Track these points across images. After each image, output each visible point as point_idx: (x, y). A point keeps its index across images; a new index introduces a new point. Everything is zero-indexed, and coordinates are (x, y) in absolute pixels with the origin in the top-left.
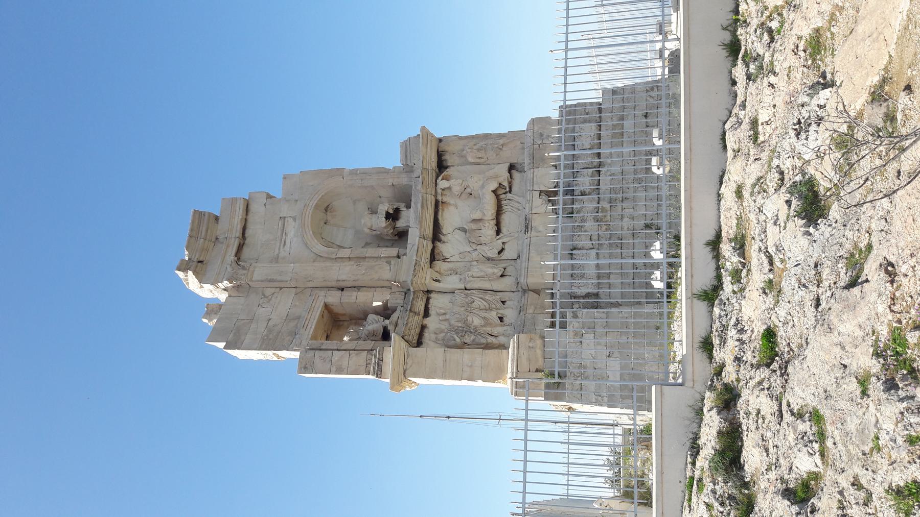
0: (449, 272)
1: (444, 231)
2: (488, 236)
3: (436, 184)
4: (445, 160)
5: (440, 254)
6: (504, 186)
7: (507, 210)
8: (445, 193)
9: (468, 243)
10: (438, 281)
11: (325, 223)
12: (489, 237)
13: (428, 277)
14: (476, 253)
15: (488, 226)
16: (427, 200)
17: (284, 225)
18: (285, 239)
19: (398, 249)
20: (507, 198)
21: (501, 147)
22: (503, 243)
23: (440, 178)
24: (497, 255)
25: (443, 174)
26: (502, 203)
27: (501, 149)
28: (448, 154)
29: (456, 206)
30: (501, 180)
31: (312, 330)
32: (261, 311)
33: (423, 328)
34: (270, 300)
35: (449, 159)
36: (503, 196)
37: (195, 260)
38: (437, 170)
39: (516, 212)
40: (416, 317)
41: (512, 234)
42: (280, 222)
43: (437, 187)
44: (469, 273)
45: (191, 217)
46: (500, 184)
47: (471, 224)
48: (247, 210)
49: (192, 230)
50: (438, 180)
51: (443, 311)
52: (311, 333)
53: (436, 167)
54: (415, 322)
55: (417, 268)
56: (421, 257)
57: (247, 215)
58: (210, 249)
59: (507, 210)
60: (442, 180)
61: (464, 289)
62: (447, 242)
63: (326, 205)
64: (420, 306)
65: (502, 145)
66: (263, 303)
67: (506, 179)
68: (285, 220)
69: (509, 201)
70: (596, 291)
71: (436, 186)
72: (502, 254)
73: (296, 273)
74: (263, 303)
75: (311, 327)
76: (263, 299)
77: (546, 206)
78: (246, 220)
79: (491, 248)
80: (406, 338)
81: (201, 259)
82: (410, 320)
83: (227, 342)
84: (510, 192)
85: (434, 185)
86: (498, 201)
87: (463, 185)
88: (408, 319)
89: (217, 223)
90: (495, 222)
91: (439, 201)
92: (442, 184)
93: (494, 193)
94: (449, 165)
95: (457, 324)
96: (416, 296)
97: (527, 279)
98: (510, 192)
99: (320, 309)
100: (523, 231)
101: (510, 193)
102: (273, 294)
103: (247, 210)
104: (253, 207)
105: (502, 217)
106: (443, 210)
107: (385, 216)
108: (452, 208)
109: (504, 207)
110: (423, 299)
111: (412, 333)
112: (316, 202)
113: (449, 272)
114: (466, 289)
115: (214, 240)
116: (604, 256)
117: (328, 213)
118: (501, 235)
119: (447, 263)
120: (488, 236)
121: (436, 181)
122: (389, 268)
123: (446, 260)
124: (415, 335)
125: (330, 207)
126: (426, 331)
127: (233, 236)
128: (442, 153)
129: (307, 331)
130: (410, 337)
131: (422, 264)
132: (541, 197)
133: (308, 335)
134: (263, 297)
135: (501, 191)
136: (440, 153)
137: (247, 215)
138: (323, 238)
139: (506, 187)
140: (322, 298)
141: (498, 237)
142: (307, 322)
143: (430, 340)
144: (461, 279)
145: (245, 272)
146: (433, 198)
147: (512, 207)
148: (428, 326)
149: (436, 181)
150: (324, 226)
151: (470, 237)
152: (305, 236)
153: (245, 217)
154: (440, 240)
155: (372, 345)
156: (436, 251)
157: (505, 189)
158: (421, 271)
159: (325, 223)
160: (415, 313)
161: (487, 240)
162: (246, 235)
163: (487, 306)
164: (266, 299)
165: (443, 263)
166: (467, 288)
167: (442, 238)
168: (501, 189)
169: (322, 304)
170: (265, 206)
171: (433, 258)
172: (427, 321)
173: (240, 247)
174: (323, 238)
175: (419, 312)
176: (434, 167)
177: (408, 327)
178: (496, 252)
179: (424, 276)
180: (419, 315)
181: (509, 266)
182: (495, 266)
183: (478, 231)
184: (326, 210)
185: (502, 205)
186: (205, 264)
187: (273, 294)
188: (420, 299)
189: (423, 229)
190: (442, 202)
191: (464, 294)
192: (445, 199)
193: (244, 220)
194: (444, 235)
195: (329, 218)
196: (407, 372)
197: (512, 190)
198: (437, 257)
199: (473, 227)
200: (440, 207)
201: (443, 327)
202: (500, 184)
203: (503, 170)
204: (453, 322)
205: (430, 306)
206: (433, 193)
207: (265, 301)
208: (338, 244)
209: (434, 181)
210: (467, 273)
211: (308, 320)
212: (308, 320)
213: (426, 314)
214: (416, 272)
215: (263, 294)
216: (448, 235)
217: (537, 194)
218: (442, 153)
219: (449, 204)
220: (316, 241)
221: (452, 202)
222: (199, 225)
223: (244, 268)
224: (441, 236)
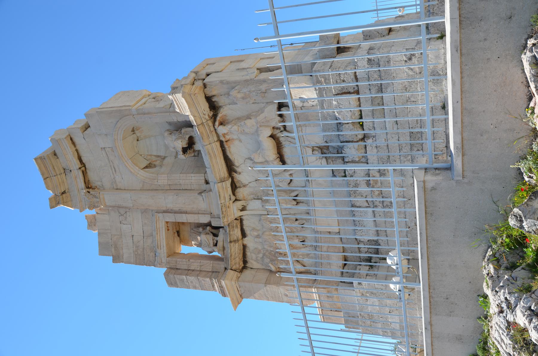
0: (252, 196)
1: (236, 164)
3: (215, 129)
4: (215, 101)
10: (243, 209)
11: (138, 140)
13: (235, 211)
16: (212, 148)
17: (107, 154)
18: (114, 166)
19: (203, 175)
21: (265, 91)
23: (217, 123)
25: (218, 118)
26: (280, 140)
27: (265, 93)
29: (240, 141)
30: (273, 124)
31: (165, 248)
32: (124, 227)
33: (244, 247)
34: (126, 218)
35: (220, 100)
37: (59, 194)
40: (236, 245)
42: (103, 152)
45: (36, 165)
46: (273, 128)
48: (74, 143)
49: (43, 174)
50: (215, 127)
51: (256, 234)
52: (165, 251)
54: (237, 250)
55: (224, 210)
56: (225, 198)
57: (75, 146)
58: (65, 180)
62: (242, 172)
63: (131, 130)
64: (237, 233)
65: (266, 90)
66: (122, 220)
68: (105, 150)
70: (375, 238)
73: (135, 201)
74: (122, 220)
75: (163, 246)
76: (121, 217)
77: (320, 161)
78: (77, 150)
80: (234, 268)
81: (63, 191)
82: (233, 250)
83: (112, 256)
85: (214, 133)
87: (240, 131)
88: (231, 251)
89: (58, 158)
90: (279, 159)
92: (222, 130)
94: (220, 105)
95: (269, 249)
96: (230, 227)
99: (164, 228)
102: (126, 212)
103: (74, 143)
104: (76, 140)
105: (283, 151)
106: (229, 147)
107: (182, 153)
108: (237, 143)
109: (283, 143)
110: (237, 226)
111: (237, 261)
112: (122, 136)
113: (252, 196)
115: (62, 171)
116: (380, 215)
117: (136, 132)
122: (202, 199)
124: (240, 261)
125: (135, 127)
126: (247, 248)
127: (75, 169)
129: (162, 250)
130: (237, 265)
131: (227, 203)
132: (314, 153)
133: (164, 253)
134: (120, 215)
135: (276, 132)
137: (75, 146)
138: (141, 155)
140: (163, 219)
142: (159, 243)
143: (252, 259)
145: (98, 200)
146: (218, 144)
148: (247, 245)
150: (137, 144)
152: (127, 165)
153: (74, 149)
154: (236, 172)
155: (211, 265)
156: (235, 180)
158: (228, 209)
159: (138, 140)
160: (235, 241)
162: (84, 161)
163: (290, 231)
164: (122, 216)
167: (238, 170)
169: (164, 223)
170: (84, 139)
171: (234, 187)
172: (246, 241)
173: (84, 173)
174: (141, 155)
175: (238, 238)
176: (207, 117)
177: (233, 257)
178: (286, 184)
179: (232, 212)
180: (238, 240)
181: (300, 192)
184: (133, 131)
185: (280, 141)
186: (68, 192)
187: (126, 212)
188: (235, 228)
189: (217, 175)
191: (269, 221)
192: (228, 137)
193: (76, 152)
194: (237, 167)
195: (138, 135)
196: (242, 295)
198: (238, 185)
200: (226, 146)
201: (260, 247)
203: (272, 112)
204: (266, 247)
205: (244, 228)
206: (216, 139)
207: (123, 219)
208: (155, 154)
209: (212, 129)
211: (159, 240)
212: (159, 240)
213: (244, 235)
214: (224, 213)
215: (119, 213)
217: (310, 151)
219: (233, 139)
220: (137, 168)
221: (235, 137)
222: (46, 168)
223: (95, 197)
224: (235, 168)
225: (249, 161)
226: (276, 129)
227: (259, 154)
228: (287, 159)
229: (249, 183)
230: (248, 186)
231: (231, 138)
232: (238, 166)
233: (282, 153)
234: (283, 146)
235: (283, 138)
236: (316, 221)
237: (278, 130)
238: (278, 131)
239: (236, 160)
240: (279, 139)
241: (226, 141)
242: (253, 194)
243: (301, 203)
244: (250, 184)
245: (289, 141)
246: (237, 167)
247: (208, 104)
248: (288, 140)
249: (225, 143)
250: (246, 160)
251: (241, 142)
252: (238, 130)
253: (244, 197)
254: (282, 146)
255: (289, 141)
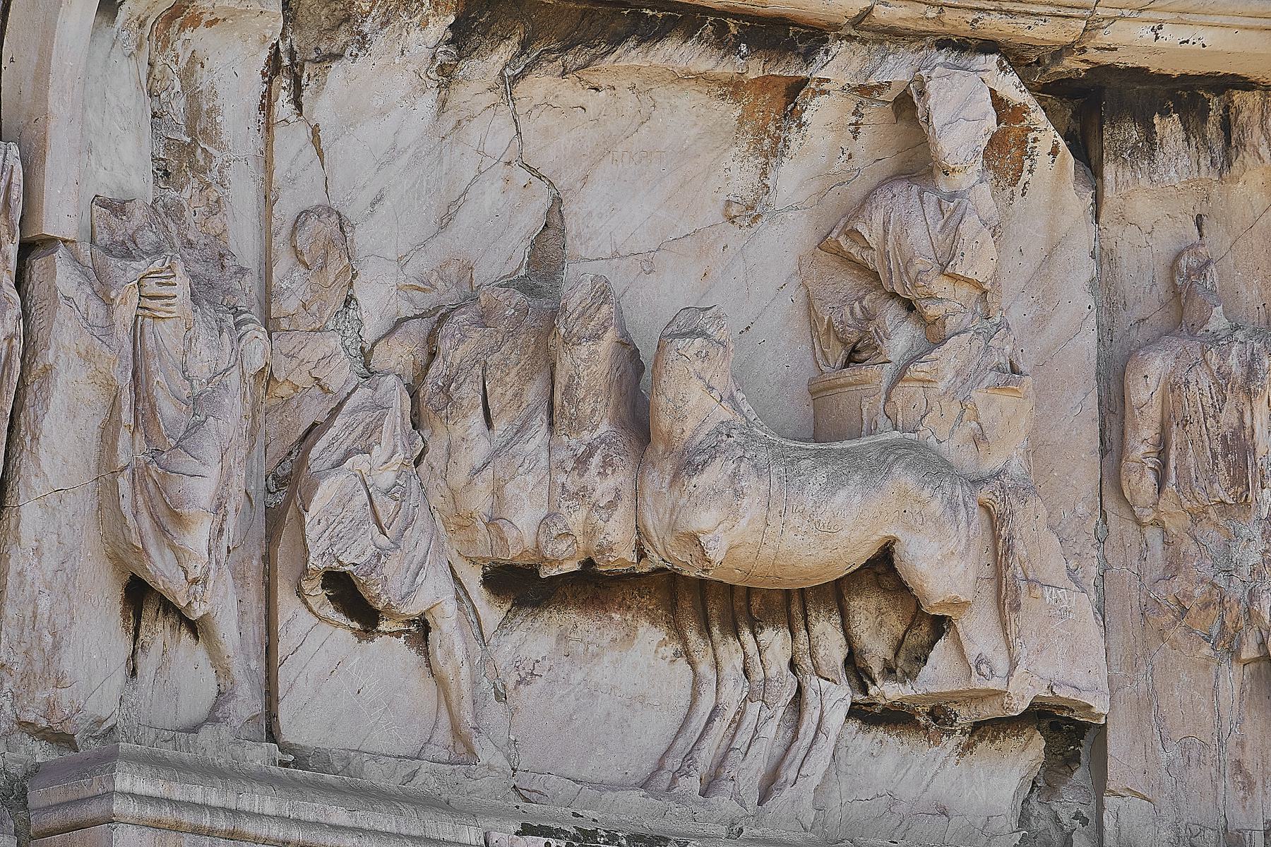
0: (179, 106)
2: (497, 493)
4: (1150, 141)
5: (342, 37)
6: (921, 659)
7: (705, 668)
8: (876, 114)
9: (425, 301)
12: (479, 501)
14: (341, 374)
15: (582, 494)
20: (813, 683)
22: (420, 631)
23: (1011, 87)
24: (317, 562)
26: (767, 635)
28: (1206, 173)
36: (832, 648)
38: (1071, 64)
39: (690, 756)
41: (495, 711)
43: (941, 57)
44: (182, 287)
47: (610, 336)
53: (1107, 59)
59: (705, 668)
60: (998, 102)
61: (32, 234)
67: (978, 683)
69: (788, 693)
71: (944, 43)
72: (329, 611)
79: (386, 507)
84: (862, 714)
86: (788, 593)
87: (940, 286)
91: (808, 57)
93: (871, 564)
94: (1109, 171)
97: (140, 823)
98: (862, 714)
100: (537, 813)
101: (855, 712)
106: (734, 88)
114: (28, 248)
118: (491, 612)
119: (257, 86)
120: (497, 493)
121: (988, 46)
123: (284, 81)
128: (1214, 117)
136: (1215, 103)
139: (910, 676)
141: (473, 578)
144: (117, 207)
147: (737, 723)
149: (988, 46)
151: (483, 320)
157: (889, 671)
161: (459, 478)
165: (265, 55)
166: (38, 265)
168: (895, 624)
178: (351, 558)
182: (225, 542)
183: (534, 392)
190: (802, 83)
194: (509, 82)
197: (879, 733)
199: (583, 350)
200: (755, 69)
202: (940, 626)
210: (179, 269)
216: (502, 122)
218: (1214, 117)
224: (504, 52)
225: (530, 219)
226: (900, 629)
227: (736, 407)
228: (562, 637)
229: (315, 131)
230: (283, 106)
231: (793, 135)
232: (521, 87)
233: (624, 607)
234: (693, 636)
235: (785, 663)
236: (197, 831)
237: (890, 656)
238: (877, 650)
239: (590, 98)
240: (774, 625)
241: (797, 86)
242: (191, 132)
243: (125, 646)
244: (304, 134)
245: (741, 712)
246: (509, 82)
247: (1164, 78)
248: (754, 709)
249: (791, 69)
250: (542, 201)
251: (732, 220)
252: (954, 278)
253: (195, 21)
254: (705, 631)
255: (741, 712)
